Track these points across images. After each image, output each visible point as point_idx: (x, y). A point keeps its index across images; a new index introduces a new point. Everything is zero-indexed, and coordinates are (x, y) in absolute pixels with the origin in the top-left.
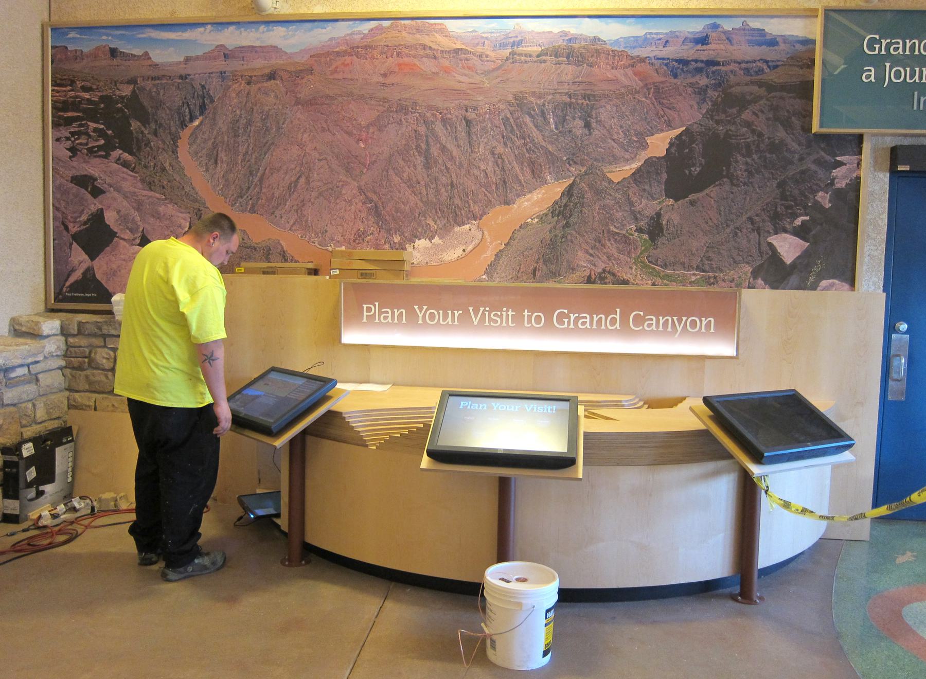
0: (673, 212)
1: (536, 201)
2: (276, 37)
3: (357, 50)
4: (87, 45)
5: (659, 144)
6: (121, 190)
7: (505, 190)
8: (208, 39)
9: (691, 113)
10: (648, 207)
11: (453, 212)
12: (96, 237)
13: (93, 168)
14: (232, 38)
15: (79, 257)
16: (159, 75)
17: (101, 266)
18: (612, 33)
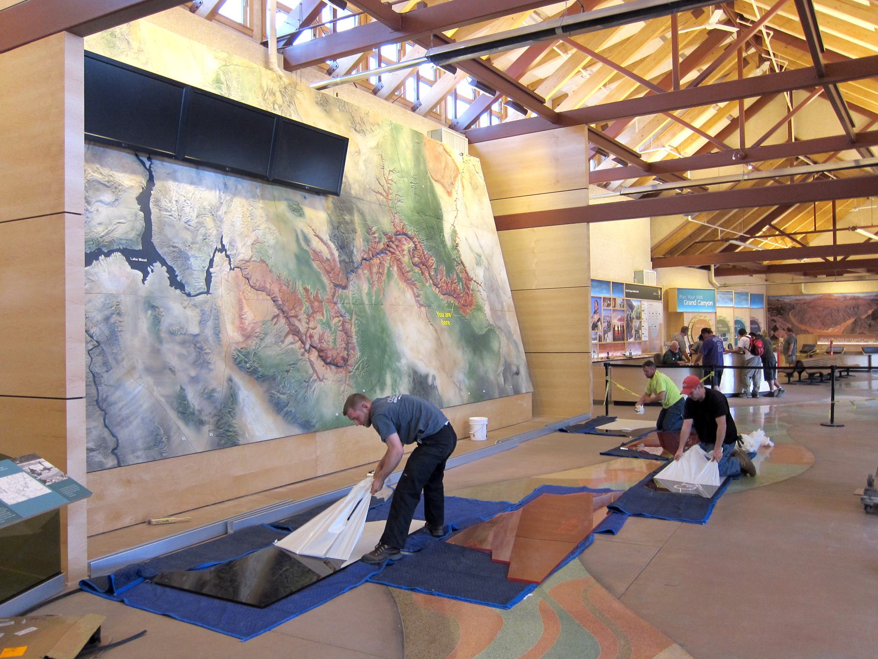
0: (873, 323)
1: (850, 321)
2: (806, 297)
3: (820, 299)
4: (773, 299)
5: (870, 312)
6: (780, 322)
7: (845, 320)
8: (794, 298)
9: (874, 307)
10: (869, 322)
11: (836, 323)
12: (775, 329)
13: (775, 318)
14: (798, 298)
15: (772, 332)
16: (785, 303)
17: (776, 334)
18: (861, 295)
